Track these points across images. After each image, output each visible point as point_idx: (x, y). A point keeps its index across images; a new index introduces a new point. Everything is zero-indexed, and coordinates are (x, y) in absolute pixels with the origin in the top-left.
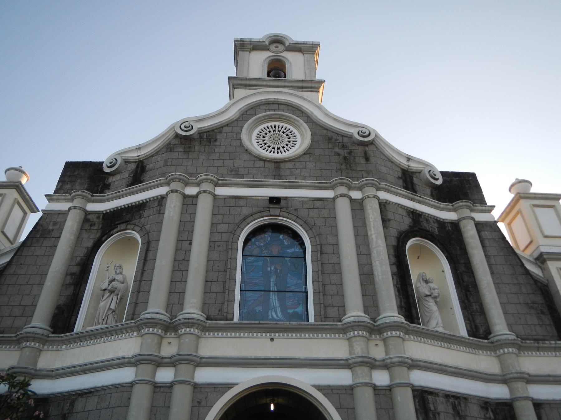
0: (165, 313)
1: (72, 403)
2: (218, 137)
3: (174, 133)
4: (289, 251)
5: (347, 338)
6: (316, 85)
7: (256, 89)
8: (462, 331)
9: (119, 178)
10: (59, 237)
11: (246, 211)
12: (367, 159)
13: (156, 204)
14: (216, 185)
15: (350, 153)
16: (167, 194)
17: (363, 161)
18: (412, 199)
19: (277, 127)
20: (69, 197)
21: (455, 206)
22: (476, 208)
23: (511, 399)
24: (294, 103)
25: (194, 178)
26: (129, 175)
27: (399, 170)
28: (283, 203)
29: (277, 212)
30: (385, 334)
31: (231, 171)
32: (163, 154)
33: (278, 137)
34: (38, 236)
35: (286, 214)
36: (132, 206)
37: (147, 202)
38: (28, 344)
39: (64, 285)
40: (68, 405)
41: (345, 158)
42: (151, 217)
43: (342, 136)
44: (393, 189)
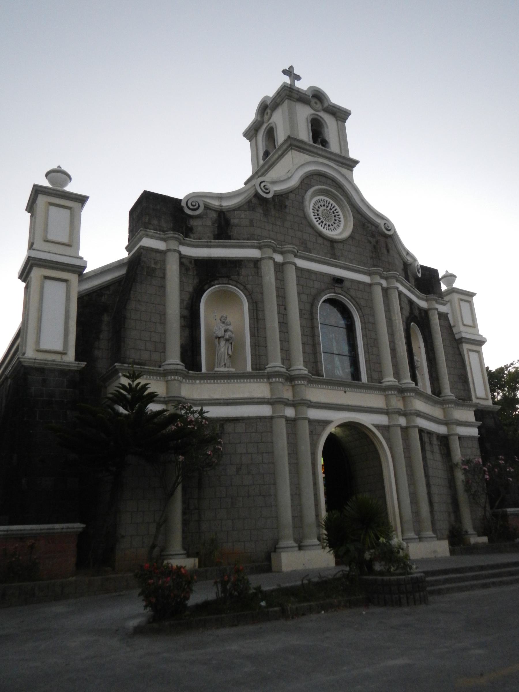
0: (282, 366)
1: (222, 426)
2: (287, 203)
5: (385, 394)
6: (351, 163)
8: (429, 391)
10: (164, 277)
11: (317, 285)
12: (388, 251)
13: (252, 265)
15: (377, 242)
16: (261, 259)
17: (385, 252)
19: (334, 209)
20: (163, 236)
21: (428, 298)
23: (448, 435)
24: (338, 180)
25: (280, 247)
26: (213, 224)
29: (338, 290)
30: (406, 394)
32: (246, 211)
33: (329, 215)
34: (145, 274)
36: (225, 260)
38: (176, 378)
39: (183, 327)
40: (218, 427)
41: (375, 247)
42: (251, 277)
43: (371, 224)
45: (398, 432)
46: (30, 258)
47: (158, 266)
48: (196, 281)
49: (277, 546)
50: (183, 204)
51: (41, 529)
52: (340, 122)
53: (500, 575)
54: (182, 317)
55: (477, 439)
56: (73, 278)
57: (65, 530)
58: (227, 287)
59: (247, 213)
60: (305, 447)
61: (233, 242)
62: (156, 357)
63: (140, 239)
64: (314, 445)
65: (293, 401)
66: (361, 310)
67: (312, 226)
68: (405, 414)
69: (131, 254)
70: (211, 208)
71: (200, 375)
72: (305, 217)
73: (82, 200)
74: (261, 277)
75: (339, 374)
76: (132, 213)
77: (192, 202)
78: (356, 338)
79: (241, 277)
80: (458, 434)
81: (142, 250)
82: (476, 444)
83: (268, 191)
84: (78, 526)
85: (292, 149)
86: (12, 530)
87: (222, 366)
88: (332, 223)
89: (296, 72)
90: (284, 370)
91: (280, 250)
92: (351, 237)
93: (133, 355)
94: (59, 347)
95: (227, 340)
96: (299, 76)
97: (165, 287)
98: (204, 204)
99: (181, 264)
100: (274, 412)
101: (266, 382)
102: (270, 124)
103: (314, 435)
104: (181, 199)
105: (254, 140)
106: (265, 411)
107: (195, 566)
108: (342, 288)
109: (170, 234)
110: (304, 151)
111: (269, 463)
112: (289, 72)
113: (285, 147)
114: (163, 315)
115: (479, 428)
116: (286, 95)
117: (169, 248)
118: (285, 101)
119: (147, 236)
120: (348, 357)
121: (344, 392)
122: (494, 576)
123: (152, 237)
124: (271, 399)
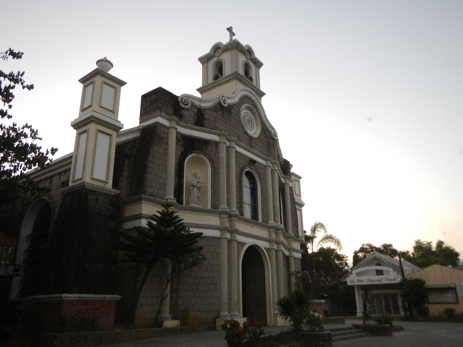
3: (218, 101)
6: (262, 95)
7: (245, 86)
9: (187, 113)
10: (167, 144)
11: (243, 162)
12: (274, 149)
13: (214, 145)
17: (272, 148)
25: (229, 137)
26: (194, 115)
29: (253, 167)
32: (213, 112)
37: (209, 141)
41: (268, 145)
43: (268, 131)
45: (274, 253)
46: (92, 117)
47: (165, 136)
48: (183, 149)
49: (219, 315)
50: (180, 100)
51: (98, 298)
52: (257, 69)
53: (345, 334)
54: (176, 170)
55: (300, 260)
56: (114, 133)
57: (110, 299)
58: (200, 155)
59: (214, 113)
60: (235, 257)
61: (205, 129)
62: (161, 193)
63: (156, 116)
65: (231, 229)
66: (261, 181)
67: (243, 128)
68: (277, 243)
69: (146, 124)
70: (195, 106)
71: (183, 208)
72: (240, 121)
73: (122, 83)
74: (219, 153)
76: (144, 97)
77: (185, 100)
78: (257, 196)
79: (208, 151)
80: (293, 256)
81: (157, 124)
82: (299, 262)
83: (225, 102)
84: (117, 297)
85: (236, 79)
86: (82, 297)
87: (194, 203)
88: (250, 127)
89: (234, 31)
90: (228, 210)
91: (229, 138)
92: (259, 137)
93: (150, 190)
94: (103, 178)
95: (198, 188)
96: (234, 34)
97: (167, 150)
98: (192, 103)
99: (177, 137)
100: (221, 235)
101: (218, 217)
102: (220, 59)
104: (178, 96)
105: (206, 65)
106: (217, 233)
107: (178, 325)
108: (254, 166)
109: (174, 118)
110: (242, 82)
111: (217, 265)
112: (230, 29)
113: (231, 77)
114: (166, 167)
115: (302, 254)
116: (235, 47)
117: (171, 126)
118: (234, 49)
119: (161, 116)
120: (250, 206)
121: (251, 227)
122: (345, 334)
123: (163, 117)
124: (221, 227)
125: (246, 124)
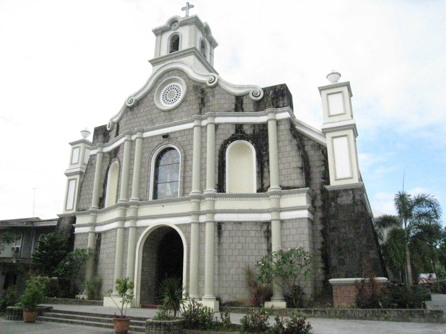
4: (176, 160)
11: (156, 144)
14: (143, 131)
18: (238, 116)
22: (278, 111)
27: (234, 98)
28: (171, 136)
29: (167, 142)
31: (150, 121)
35: (171, 142)
44: (223, 114)
64: (136, 241)
75: (168, 194)
103: (137, 235)
125: (176, 98)
